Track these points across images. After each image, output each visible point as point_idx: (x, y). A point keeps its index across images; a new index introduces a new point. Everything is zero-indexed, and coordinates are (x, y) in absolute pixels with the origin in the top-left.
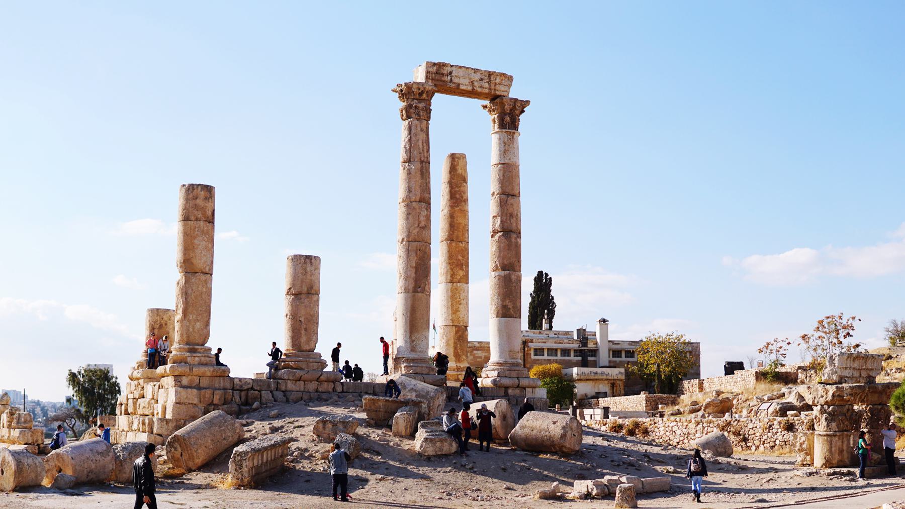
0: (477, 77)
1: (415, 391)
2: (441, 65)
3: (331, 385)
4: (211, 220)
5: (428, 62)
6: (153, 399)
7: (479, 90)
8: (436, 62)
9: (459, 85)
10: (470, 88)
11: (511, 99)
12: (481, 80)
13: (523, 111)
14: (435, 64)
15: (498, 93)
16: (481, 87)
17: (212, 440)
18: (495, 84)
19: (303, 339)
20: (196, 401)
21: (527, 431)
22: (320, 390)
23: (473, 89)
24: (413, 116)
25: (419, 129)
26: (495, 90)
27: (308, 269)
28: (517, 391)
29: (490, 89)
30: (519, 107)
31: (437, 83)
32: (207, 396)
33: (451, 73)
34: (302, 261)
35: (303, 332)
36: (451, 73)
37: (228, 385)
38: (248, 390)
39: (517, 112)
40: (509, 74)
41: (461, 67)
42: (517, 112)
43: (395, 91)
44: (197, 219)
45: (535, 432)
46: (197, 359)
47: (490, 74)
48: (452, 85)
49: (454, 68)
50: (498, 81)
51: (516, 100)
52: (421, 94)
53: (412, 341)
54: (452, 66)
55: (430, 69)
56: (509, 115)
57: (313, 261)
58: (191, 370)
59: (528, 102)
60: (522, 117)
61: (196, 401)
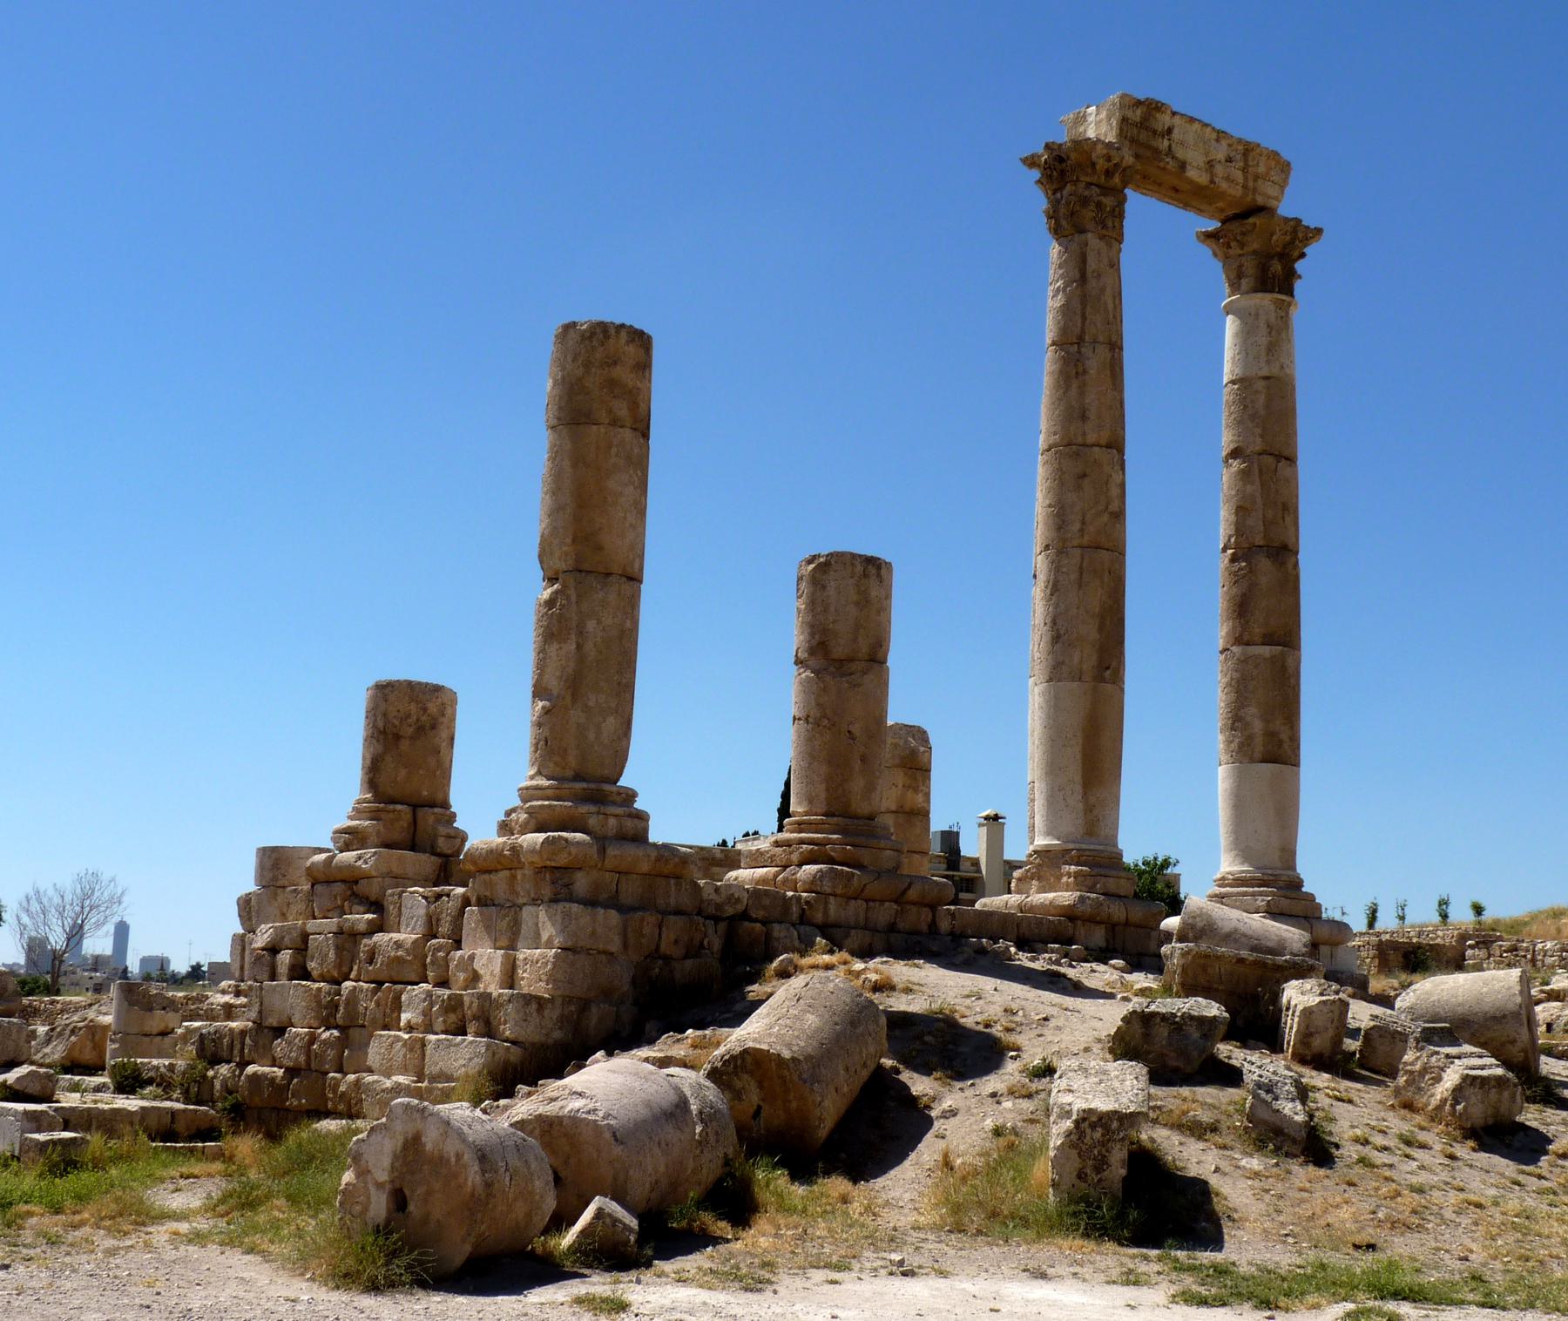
0: (1220, 153)
2: (1153, 107)
3: (926, 915)
4: (642, 429)
5: (1123, 96)
7: (1224, 185)
8: (1142, 97)
11: (1287, 220)
12: (1229, 160)
13: (1303, 255)
14: (1139, 103)
15: (1260, 200)
16: (1228, 179)
17: (847, 1069)
18: (1256, 177)
19: (857, 784)
20: (615, 946)
22: (901, 925)
23: (1212, 182)
24: (1090, 225)
25: (1106, 261)
26: (1255, 190)
27: (874, 593)
29: (1245, 187)
30: (1299, 236)
32: (647, 930)
34: (859, 568)
35: (857, 765)
36: (1170, 131)
37: (686, 901)
38: (733, 919)
40: (1286, 155)
41: (1192, 120)
42: (1296, 254)
43: (1031, 162)
44: (615, 422)
46: (612, 821)
47: (1248, 149)
49: (1177, 120)
50: (1261, 169)
51: (1298, 221)
52: (1108, 173)
53: (1089, 809)
54: (1174, 114)
55: (1129, 114)
56: (1266, 256)
57: (883, 572)
58: (602, 851)
59: (1319, 231)
60: (1300, 266)
61: (615, 946)
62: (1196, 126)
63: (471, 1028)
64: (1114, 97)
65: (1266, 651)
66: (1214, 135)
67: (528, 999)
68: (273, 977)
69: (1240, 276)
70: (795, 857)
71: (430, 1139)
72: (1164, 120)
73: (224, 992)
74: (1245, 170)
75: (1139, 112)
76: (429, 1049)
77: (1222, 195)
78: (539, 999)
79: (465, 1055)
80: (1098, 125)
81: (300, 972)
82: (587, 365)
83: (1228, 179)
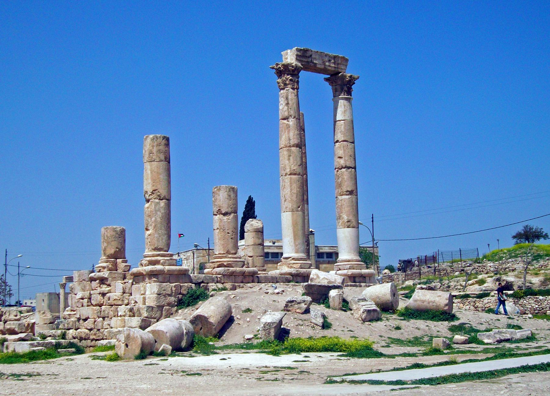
1: (327, 279)
2: (305, 51)
6: (124, 293)
10: (322, 67)
13: (354, 83)
18: (338, 64)
21: (419, 303)
26: (338, 68)
34: (228, 190)
36: (311, 56)
39: (351, 84)
42: (351, 84)
45: (425, 303)
47: (335, 57)
48: (312, 65)
50: (340, 62)
63: (136, 315)
64: (295, 49)
65: (347, 197)
67: (149, 307)
68: (82, 306)
69: (336, 91)
70: (216, 266)
71: (132, 333)
72: (309, 54)
73: (67, 311)
74: (334, 63)
76: (126, 321)
77: (329, 70)
78: (152, 308)
79: (136, 321)
80: (290, 57)
81: (90, 304)
82: (153, 146)
83: (329, 66)
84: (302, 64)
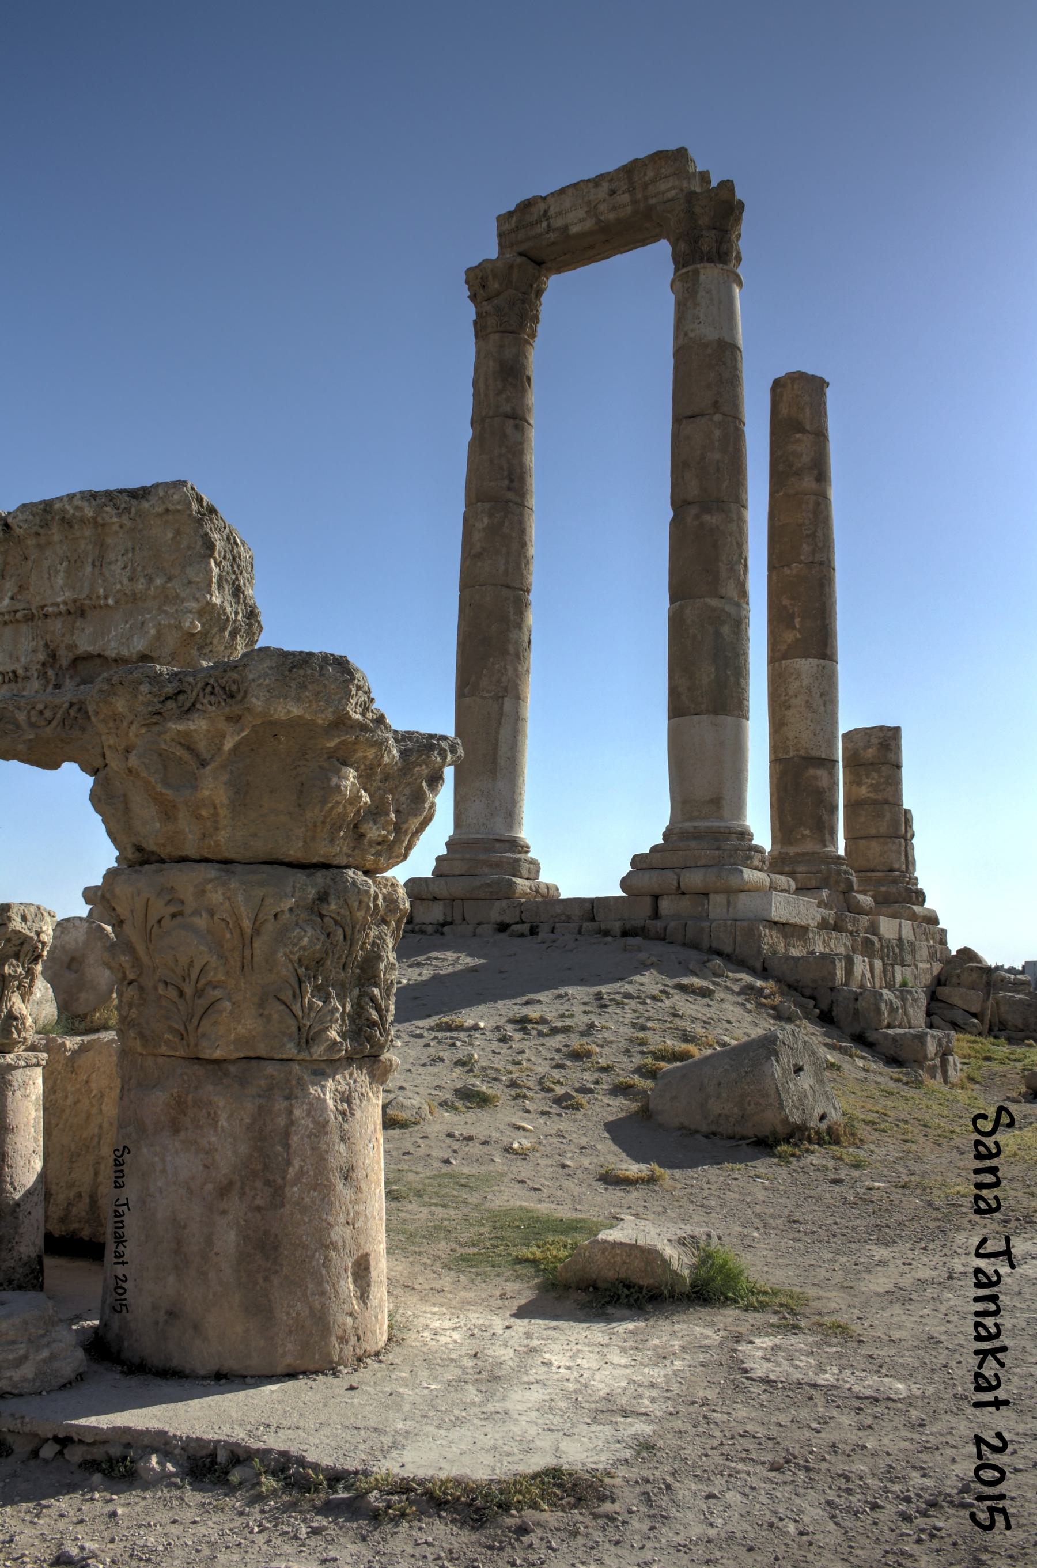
7: (611, 216)
8: (512, 208)
9: (566, 228)
12: (612, 193)
14: (510, 214)
16: (614, 208)
28: (685, 903)
29: (634, 202)
31: (523, 248)
33: (546, 212)
36: (546, 212)
40: (672, 146)
41: (562, 191)
47: (630, 170)
48: (552, 236)
50: (650, 174)
54: (544, 199)
55: (506, 227)
62: (570, 191)
66: (591, 185)
74: (631, 190)
75: (514, 220)
84: (521, 254)
